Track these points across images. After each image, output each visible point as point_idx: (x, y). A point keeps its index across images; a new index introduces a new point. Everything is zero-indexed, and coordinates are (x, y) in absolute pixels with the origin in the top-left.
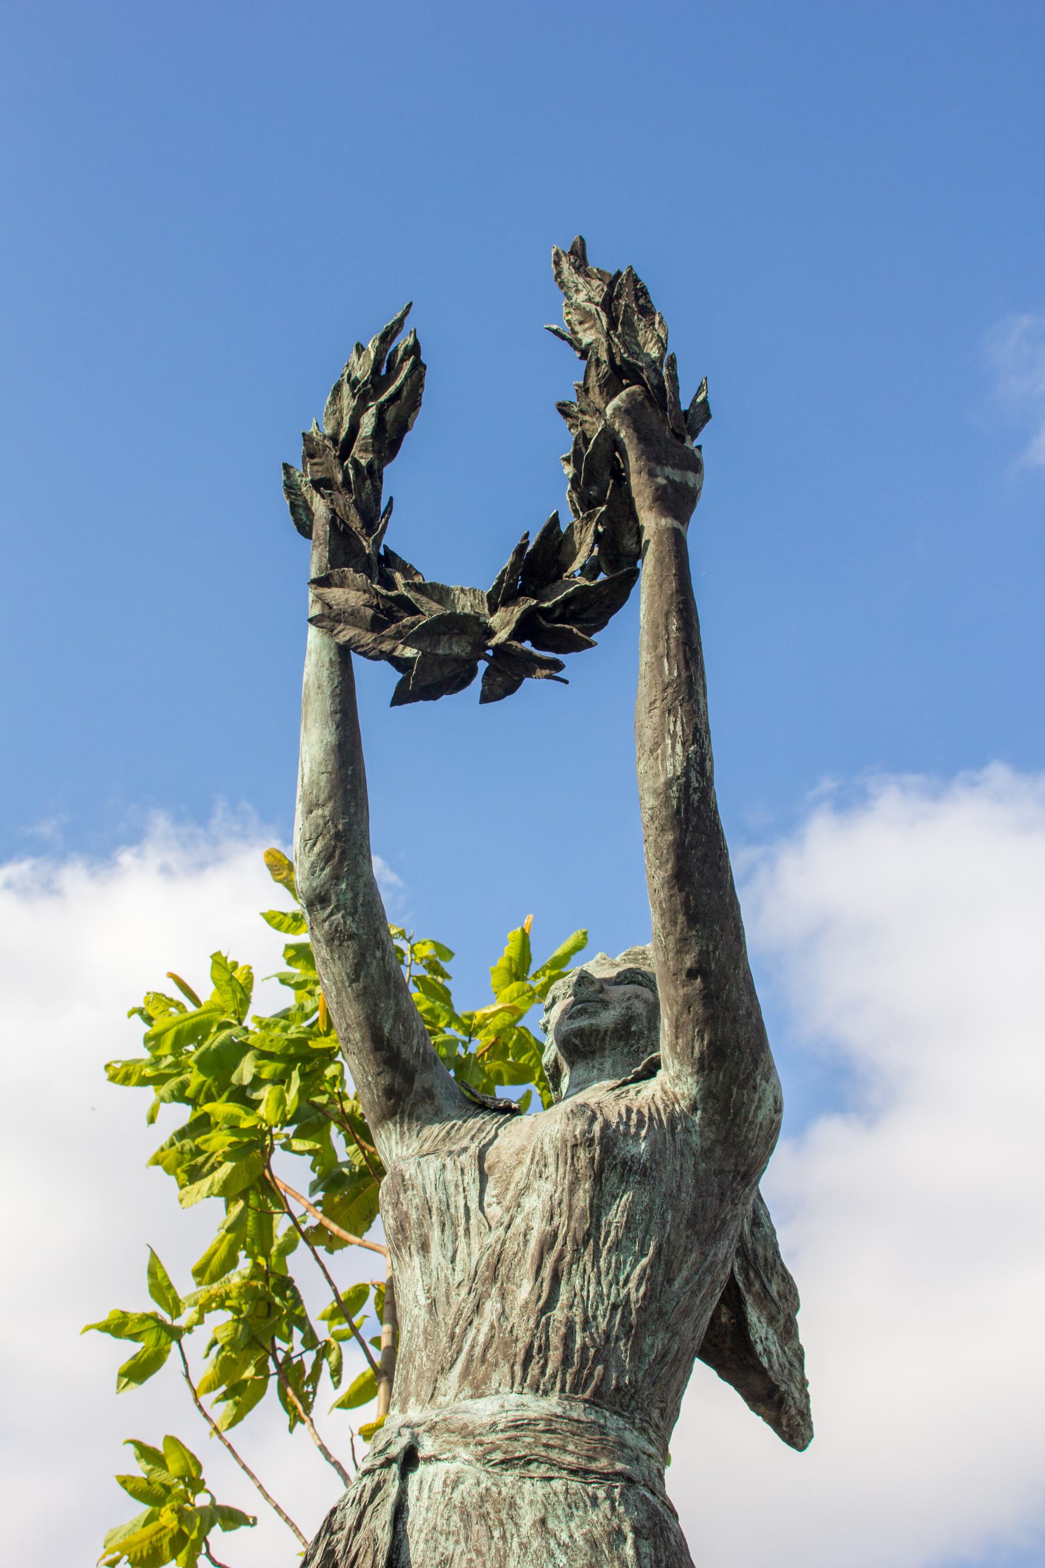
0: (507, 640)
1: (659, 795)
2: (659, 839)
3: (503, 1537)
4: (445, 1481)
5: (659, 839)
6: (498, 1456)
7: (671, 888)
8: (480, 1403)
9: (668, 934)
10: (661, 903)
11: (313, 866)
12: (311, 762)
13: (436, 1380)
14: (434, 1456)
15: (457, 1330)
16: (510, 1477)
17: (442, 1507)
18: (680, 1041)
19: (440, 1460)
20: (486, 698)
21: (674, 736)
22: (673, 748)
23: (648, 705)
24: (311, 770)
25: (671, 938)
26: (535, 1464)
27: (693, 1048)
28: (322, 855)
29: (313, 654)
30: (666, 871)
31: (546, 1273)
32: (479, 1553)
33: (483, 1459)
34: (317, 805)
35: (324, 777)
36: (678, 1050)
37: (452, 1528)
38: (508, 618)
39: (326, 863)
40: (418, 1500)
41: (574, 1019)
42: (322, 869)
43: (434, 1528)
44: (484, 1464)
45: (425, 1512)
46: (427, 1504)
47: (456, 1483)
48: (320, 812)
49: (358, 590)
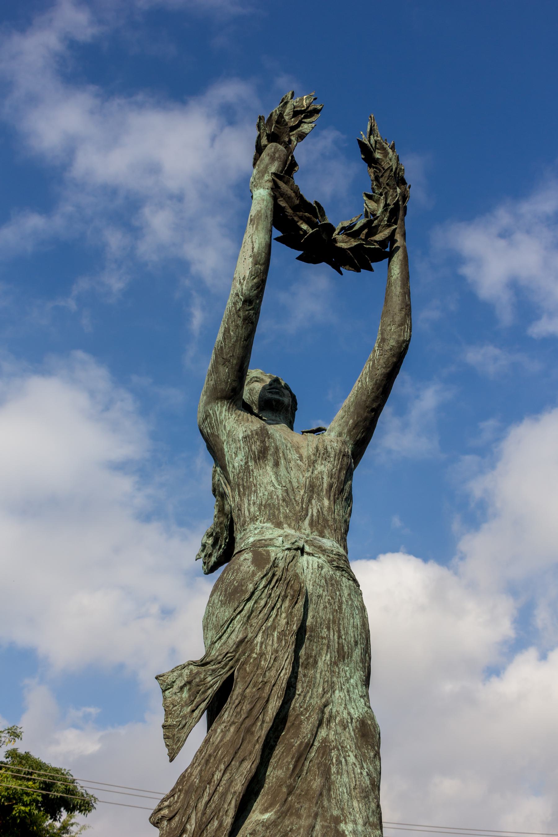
0: (347, 249)
1: (398, 343)
2: (390, 358)
3: (340, 595)
4: (318, 565)
5: (390, 358)
6: (335, 564)
7: (384, 377)
8: (324, 540)
9: (373, 392)
10: (377, 380)
11: (252, 286)
12: (259, 244)
13: (299, 523)
14: (312, 554)
15: (304, 506)
16: (338, 573)
17: (318, 575)
18: (354, 431)
19: (314, 556)
20: (300, 258)
21: (408, 325)
22: (407, 329)
23: (400, 308)
24: (259, 248)
25: (374, 394)
26: (345, 572)
27: (358, 435)
28: (257, 285)
29: (265, 202)
30: (386, 370)
31: (332, 498)
32: (332, 598)
33: (331, 562)
34: (259, 264)
35: (264, 254)
36: (352, 433)
37: (322, 585)
38: (346, 240)
39: (257, 289)
40: (307, 568)
41: (273, 394)
42: (255, 290)
43: (315, 581)
44: (331, 565)
45: (311, 574)
46: (311, 571)
47: (322, 568)
48: (260, 267)
49: (292, 190)
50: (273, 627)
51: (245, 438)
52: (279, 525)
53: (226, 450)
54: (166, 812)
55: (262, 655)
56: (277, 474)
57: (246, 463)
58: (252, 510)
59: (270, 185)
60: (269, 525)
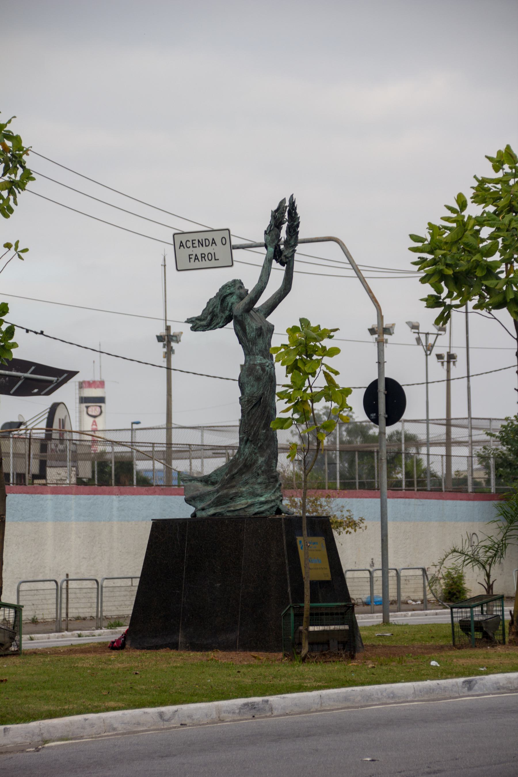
50: (268, 390)
51: (256, 329)
52: (265, 358)
53: (247, 328)
54: (246, 430)
55: (266, 397)
56: (263, 341)
57: (255, 336)
58: (257, 351)
59: (274, 247)
60: (262, 357)
